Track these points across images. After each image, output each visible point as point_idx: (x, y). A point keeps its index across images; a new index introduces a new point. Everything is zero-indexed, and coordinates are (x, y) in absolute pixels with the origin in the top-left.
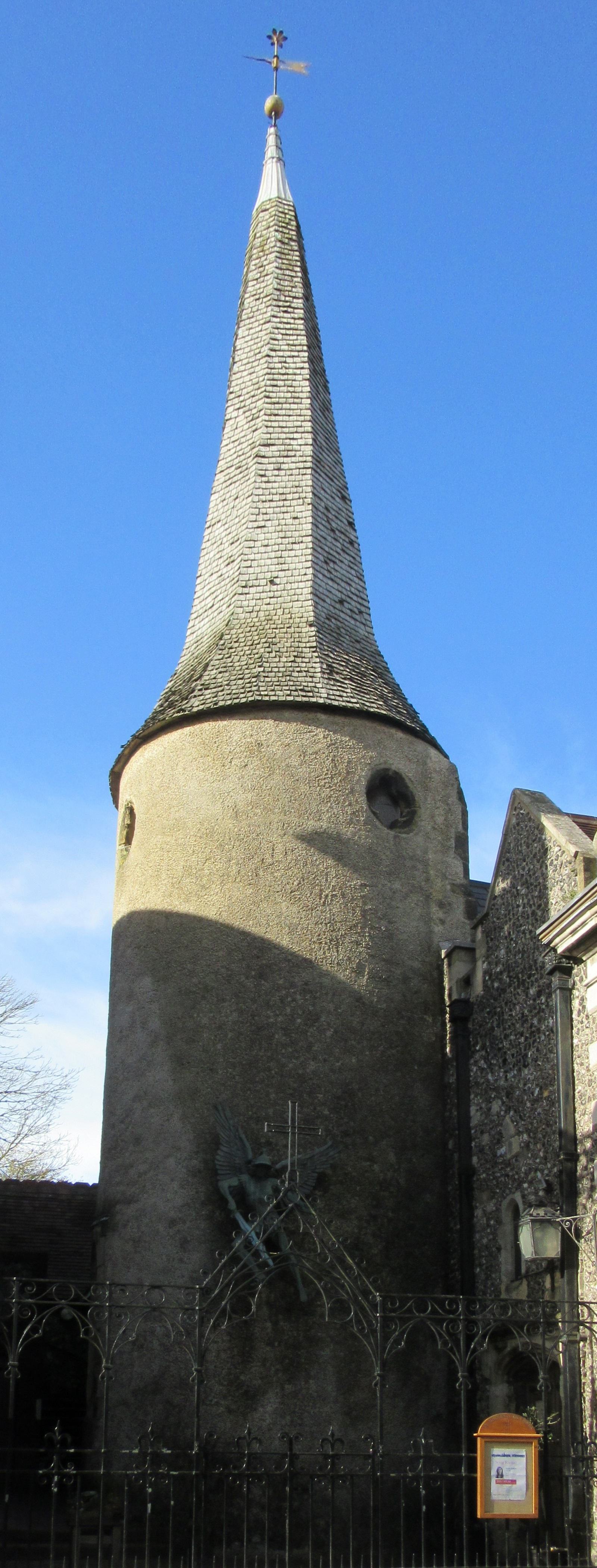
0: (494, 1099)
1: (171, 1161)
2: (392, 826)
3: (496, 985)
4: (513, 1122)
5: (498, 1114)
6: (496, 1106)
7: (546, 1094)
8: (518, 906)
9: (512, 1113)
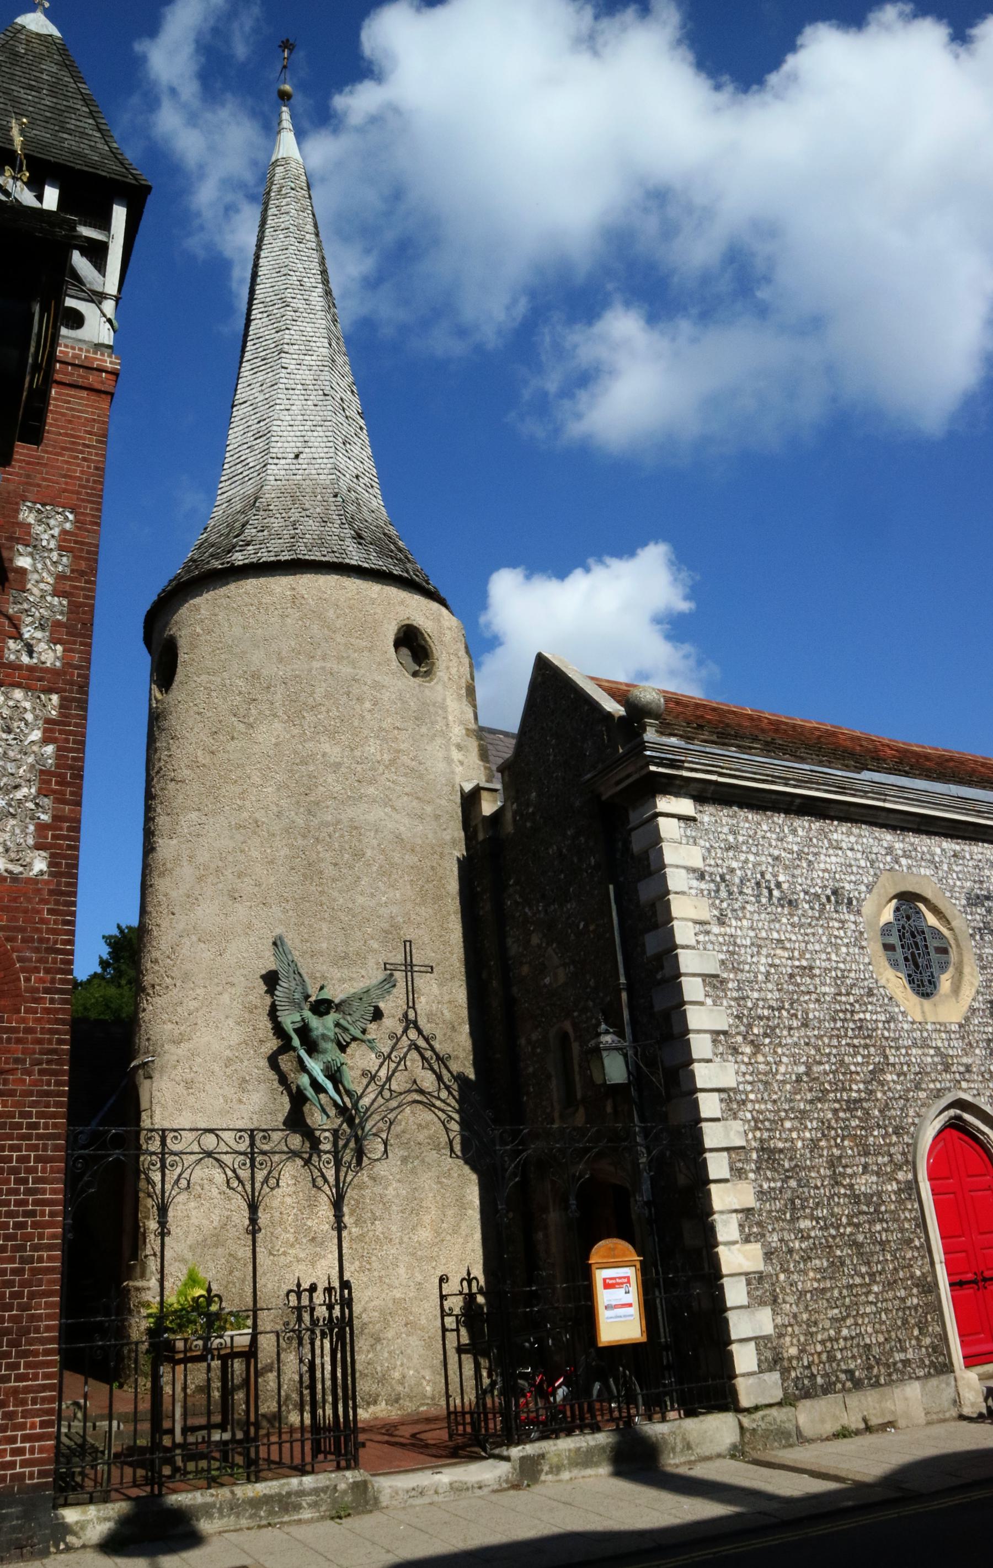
0: (533, 931)
1: (226, 998)
2: (415, 674)
3: (528, 824)
4: (556, 954)
5: (539, 946)
6: (535, 940)
7: (592, 928)
8: (549, 755)
9: (554, 945)
